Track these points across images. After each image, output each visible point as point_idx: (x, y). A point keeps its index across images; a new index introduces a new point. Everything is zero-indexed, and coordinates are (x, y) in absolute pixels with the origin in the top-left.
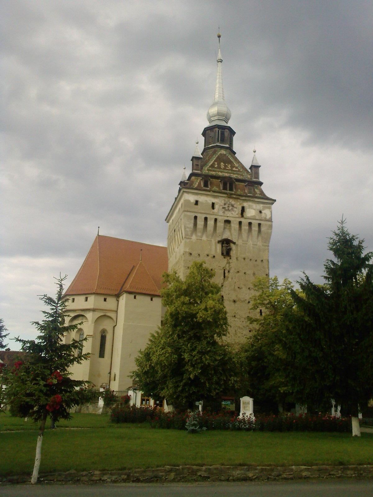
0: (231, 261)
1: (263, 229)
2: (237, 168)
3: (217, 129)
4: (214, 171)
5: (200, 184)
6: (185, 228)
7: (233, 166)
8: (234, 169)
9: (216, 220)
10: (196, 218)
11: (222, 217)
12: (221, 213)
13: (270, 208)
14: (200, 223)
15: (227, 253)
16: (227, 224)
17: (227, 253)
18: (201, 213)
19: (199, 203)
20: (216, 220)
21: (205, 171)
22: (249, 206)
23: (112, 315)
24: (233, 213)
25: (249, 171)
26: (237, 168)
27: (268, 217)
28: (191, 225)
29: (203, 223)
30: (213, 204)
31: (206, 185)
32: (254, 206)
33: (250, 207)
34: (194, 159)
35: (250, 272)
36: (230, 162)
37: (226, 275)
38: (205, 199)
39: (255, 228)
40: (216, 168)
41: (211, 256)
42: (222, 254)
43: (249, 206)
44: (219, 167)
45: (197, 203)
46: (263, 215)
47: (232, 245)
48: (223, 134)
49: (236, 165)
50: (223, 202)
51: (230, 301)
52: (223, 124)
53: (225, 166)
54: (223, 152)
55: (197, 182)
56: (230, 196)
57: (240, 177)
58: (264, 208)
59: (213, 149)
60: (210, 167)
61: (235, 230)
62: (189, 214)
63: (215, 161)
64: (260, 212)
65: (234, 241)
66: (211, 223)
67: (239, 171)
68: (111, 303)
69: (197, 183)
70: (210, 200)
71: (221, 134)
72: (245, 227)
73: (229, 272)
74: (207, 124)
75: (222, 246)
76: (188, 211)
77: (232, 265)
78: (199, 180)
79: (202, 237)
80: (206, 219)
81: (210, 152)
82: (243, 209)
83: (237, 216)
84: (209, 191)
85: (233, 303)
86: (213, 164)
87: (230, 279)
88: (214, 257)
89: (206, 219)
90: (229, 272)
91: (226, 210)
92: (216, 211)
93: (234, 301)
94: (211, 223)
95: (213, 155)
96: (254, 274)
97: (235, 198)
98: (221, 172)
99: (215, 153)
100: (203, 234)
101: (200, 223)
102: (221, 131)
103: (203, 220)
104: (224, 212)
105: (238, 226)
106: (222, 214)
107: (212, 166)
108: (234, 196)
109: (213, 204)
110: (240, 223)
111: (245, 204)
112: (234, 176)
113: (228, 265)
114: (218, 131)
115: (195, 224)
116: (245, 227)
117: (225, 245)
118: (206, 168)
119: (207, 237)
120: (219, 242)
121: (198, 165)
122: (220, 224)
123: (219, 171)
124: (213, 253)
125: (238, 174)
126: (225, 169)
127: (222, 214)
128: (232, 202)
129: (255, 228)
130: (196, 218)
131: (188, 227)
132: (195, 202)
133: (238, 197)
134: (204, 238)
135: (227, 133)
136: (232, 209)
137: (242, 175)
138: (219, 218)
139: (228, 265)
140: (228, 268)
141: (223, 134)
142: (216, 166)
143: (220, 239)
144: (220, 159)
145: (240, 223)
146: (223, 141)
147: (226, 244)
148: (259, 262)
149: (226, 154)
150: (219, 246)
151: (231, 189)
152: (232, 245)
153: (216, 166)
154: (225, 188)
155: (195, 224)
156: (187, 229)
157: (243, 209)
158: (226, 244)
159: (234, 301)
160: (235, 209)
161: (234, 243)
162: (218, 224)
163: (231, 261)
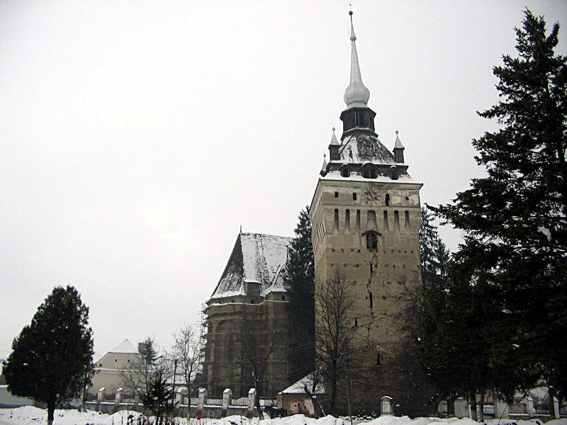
0: (377, 254)
1: (411, 217)
6: (326, 224)
9: (358, 211)
10: (336, 211)
11: (365, 208)
13: (418, 193)
14: (342, 216)
15: (372, 245)
16: (371, 214)
17: (372, 245)
18: (341, 205)
20: (358, 211)
22: (394, 193)
24: (377, 202)
25: (393, 154)
27: (416, 204)
28: (333, 219)
29: (344, 216)
30: (355, 195)
32: (400, 192)
33: (395, 194)
34: (332, 148)
35: (400, 265)
37: (373, 270)
39: (402, 217)
41: (356, 251)
42: (368, 247)
43: (394, 193)
45: (337, 194)
46: (410, 201)
47: (378, 237)
48: (362, 117)
51: (378, 297)
52: (362, 106)
58: (411, 194)
61: (379, 220)
62: (330, 207)
64: (407, 199)
65: (380, 232)
66: (353, 215)
71: (360, 117)
72: (391, 217)
73: (376, 266)
74: (345, 107)
75: (367, 239)
76: (327, 204)
77: (379, 258)
79: (344, 231)
80: (348, 211)
82: (388, 196)
85: (382, 300)
87: (377, 274)
88: (359, 251)
89: (348, 211)
90: (376, 266)
92: (357, 201)
93: (384, 298)
94: (353, 215)
96: (404, 266)
100: (345, 227)
101: (342, 216)
103: (345, 212)
104: (367, 203)
105: (383, 216)
109: (355, 195)
110: (385, 212)
111: (389, 192)
113: (375, 259)
115: (337, 218)
116: (391, 217)
117: (370, 238)
119: (349, 230)
120: (363, 235)
122: (364, 216)
124: (356, 246)
129: (402, 217)
130: (336, 211)
131: (330, 222)
134: (347, 232)
135: (366, 117)
138: (362, 209)
139: (375, 259)
140: (375, 263)
143: (362, 232)
145: (385, 212)
146: (362, 125)
147: (372, 238)
148: (409, 253)
150: (364, 239)
152: (378, 237)
155: (337, 218)
156: (329, 224)
157: (388, 196)
158: (372, 238)
159: (384, 298)
161: (381, 235)
163: (377, 254)
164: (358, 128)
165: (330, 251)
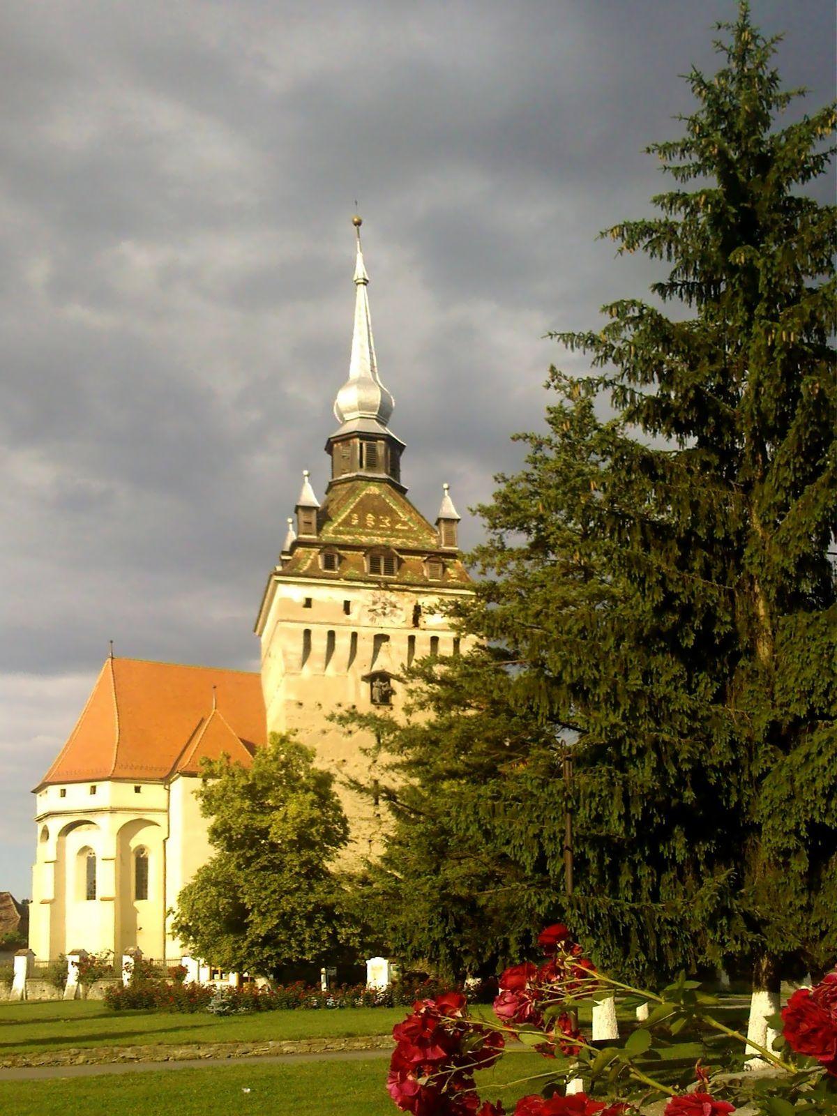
2: (404, 523)
3: (357, 441)
4: (349, 533)
5: (315, 563)
7: (395, 521)
8: (399, 526)
9: (354, 635)
10: (307, 633)
12: (366, 621)
14: (319, 644)
19: (313, 603)
20: (354, 635)
21: (329, 533)
23: (159, 818)
24: (394, 619)
26: (404, 523)
28: (299, 648)
29: (325, 643)
30: (347, 605)
31: (329, 564)
36: (391, 512)
38: (328, 596)
40: (354, 526)
44: (362, 524)
45: (308, 603)
48: (372, 450)
49: (404, 518)
50: (371, 598)
53: (377, 521)
54: (374, 489)
55: (311, 558)
56: (386, 586)
57: (412, 544)
59: (350, 485)
60: (340, 525)
63: (353, 511)
66: (343, 643)
67: (410, 530)
68: (153, 794)
69: (309, 562)
70: (340, 596)
71: (368, 450)
78: (313, 554)
80: (331, 635)
81: (342, 490)
83: (404, 625)
84: (338, 579)
86: (349, 516)
89: (331, 635)
91: (377, 615)
94: (343, 643)
95: (349, 498)
97: (398, 590)
98: (367, 535)
99: (352, 492)
101: (319, 644)
102: (367, 445)
103: (326, 636)
104: (372, 619)
105: (406, 646)
106: (369, 624)
107: (347, 522)
108: (396, 586)
109: (347, 605)
110: (412, 639)
112: (398, 542)
114: (361, 444)
118: (331, 528)
121: (310, 523)
122: (365, 646)
123: (360, 534)
125: (408, 538)
126: (376, 527)
127: (369, 624)
128: (392, 597)
130: (307, 633)
131: (292, 653)
132: (304, 602)
133: (405, 586)
136: (391, 611)
137: (417, 539)
138: (362, 632)
141: (372, 450)
142: (355, 522)
144: (363, 508)
145: (412, 639)
149: (380, 495)
151: (389, 570)
153: (355, 522)
154: (375, 569)
160: (398, 612)
162: (360, 643)
164: (362, 473)
165: (294, 710)
